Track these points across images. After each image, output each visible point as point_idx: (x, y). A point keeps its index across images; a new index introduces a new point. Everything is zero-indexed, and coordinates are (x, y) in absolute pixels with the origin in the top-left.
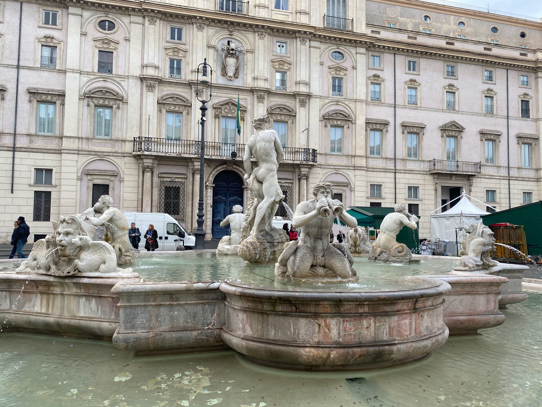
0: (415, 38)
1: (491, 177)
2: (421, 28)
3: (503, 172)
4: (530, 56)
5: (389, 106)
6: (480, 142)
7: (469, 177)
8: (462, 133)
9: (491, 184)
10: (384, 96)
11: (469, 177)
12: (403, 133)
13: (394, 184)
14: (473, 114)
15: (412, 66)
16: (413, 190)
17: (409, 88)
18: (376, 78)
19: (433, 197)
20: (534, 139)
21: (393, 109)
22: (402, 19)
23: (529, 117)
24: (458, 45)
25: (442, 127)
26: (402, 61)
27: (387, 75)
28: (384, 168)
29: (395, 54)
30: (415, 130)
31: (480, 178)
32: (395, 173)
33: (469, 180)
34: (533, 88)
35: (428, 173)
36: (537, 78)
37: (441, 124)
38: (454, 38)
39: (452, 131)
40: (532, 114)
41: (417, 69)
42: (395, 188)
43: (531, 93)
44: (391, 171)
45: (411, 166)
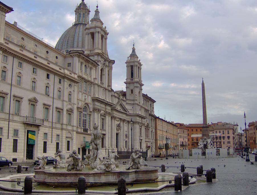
0: (22, 51)
1: (46, 127)
2: (20, 43)
3: (50, 125)
4: (62, 71)
5: (9, 84)
6: (43, 108)
7: (38, 126)
8: (37, 103)
9: (46, 130)
10: (7, 79)
11: (38, 126)
12: (14, 100)
13: (8, 128)
14: (42, 94)
15: (20, 65)
16: (16, 132)
17: (18, 76)
18: (4, 68)
19: (23, 136)
20: (61, 109)
21: (10, 86)
22: (13, 36)
23: (60, 99)
24: (38, 59)
25: (30, 99)
26: (16, 61)
27: (9, 67)
28: (4, 118)
29: (14, 57)
30: (19, 99)
31: (42, 127)
32: (9, 122)
33: (38, 128)
34: (62, 85)
35: (23, 123)
36: (64, 81)
37: (29, 98)
38: (37, 55)
39: (33, 102)
40: (62, 99)
41: (22, 67)
42: (9, 130)
43: (62, 88)
44: (7, 120)
45: (16, 118)
